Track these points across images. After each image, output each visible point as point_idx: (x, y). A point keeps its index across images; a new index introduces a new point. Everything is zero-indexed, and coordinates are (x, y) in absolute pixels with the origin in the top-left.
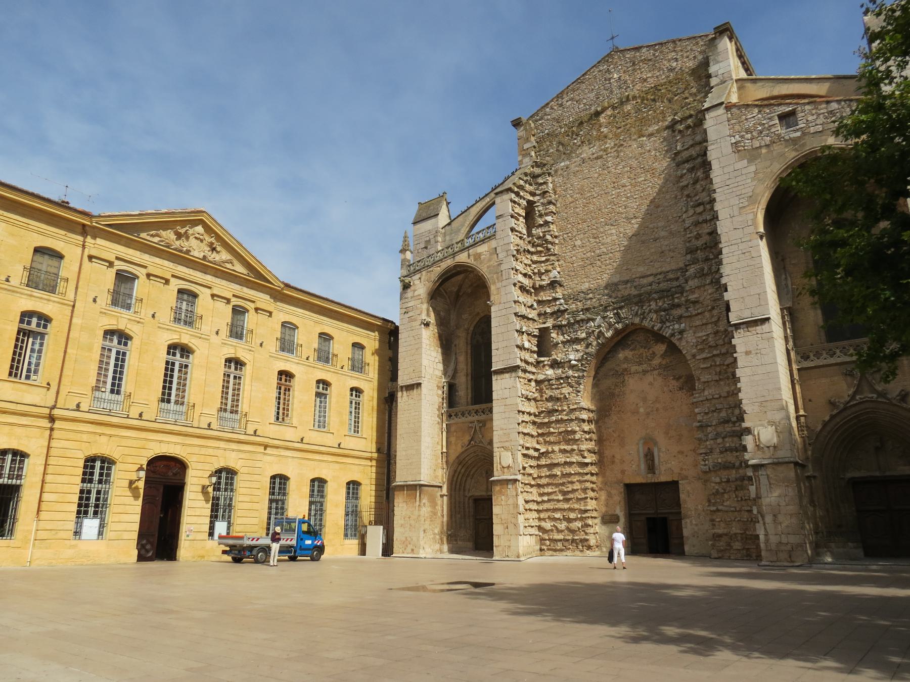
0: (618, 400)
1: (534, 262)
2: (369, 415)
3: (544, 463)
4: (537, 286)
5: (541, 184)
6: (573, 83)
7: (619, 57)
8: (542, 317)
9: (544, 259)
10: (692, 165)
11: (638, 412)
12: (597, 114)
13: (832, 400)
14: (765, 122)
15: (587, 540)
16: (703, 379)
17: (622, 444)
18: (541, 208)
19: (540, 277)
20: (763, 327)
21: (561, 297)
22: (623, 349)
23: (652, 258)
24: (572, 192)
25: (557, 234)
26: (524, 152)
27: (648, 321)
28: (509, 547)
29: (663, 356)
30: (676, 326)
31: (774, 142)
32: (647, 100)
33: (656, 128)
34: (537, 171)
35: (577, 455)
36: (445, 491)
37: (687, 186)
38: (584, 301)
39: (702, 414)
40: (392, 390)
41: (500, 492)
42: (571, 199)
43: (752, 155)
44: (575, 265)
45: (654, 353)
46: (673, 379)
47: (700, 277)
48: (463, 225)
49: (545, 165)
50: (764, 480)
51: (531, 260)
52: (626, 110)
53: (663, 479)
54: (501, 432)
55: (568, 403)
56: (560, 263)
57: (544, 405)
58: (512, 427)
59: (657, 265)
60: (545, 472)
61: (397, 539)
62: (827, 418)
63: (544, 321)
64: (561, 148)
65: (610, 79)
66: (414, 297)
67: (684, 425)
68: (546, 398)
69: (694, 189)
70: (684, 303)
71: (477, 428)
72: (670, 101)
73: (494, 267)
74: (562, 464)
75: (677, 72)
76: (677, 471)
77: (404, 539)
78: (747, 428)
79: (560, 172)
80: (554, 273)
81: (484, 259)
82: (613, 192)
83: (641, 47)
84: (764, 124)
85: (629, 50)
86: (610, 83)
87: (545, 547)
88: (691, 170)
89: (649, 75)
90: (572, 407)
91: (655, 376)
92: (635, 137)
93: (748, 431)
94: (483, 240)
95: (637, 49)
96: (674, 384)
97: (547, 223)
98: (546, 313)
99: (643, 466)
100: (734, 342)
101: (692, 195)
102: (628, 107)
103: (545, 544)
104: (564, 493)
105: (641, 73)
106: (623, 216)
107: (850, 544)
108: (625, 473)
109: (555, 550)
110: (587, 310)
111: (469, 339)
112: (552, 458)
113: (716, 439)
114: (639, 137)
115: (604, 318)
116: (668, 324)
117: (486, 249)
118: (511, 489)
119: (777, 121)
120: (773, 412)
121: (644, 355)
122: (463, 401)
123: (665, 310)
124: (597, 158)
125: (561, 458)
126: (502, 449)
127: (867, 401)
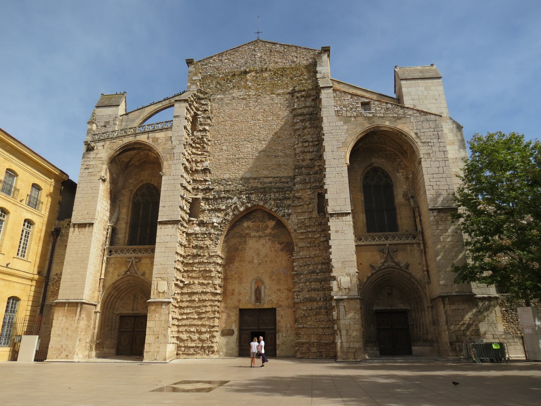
0: (240, 253)
1: (194, 154)
2: (36, 243)
3: (186, 292)
4: (194, 170)
5: (204, 105)
6: (230, 50)
7: (262, 45)
8: (195, 191)
9: (200, 153)
10: (303, 118)
11: (253, 262)
12: (246, 73)
13: (373, 265)
14: (354, 104)
15: (212, 347)
16: (300, 246)
17: (241, 282)
18: (201, 120)
19: (196, 164)
20: (347, 217)
21: (209, 180)
22: (247, 221)
23: (273, 167)
24: (223, 115)
25: (210, 139)
26: (192, 81)
27: (268, 205)
28: (158, 352)
29: (273, 229)
30: (286, 211)
31: (358, 116)
33: (282, 92)
34: (201, 96)
35: (211, 287)
36: (98, 309)
37: (299, 129)
38: (225, 185)
39: (298, 267)
40: (58, 227)
41: (155, 311)
42: (222, 119)
43: (347, 120)
44: (220, 161)
45: (267, 226)
46: (278, 244)
47: (303, 183)
48: (138, 118)
49: (206, 93)
51: (192, 152)
52: (264, 76)
53: (266, 306)
54: (160, 267)
55: (209, 251)
56: (210, 158)
57: (190, 251)
58: (170, 263)
59: (275, 172)
60: (186, 298)
62: (369, 275)
63: (196, 193)
64: (218, 86)
65: (255, 55)
67: (282, 273)
68: (192, 246)
69: (303, 132)
70: (292, 197)
71: (134, 262)
72: (291, 79)
73: (168, 149)
74: (199, 293)
75: (296, 64)
76: (275, 302)
77: (60, 346)
78: (333, 277)
81: (161, 143)
82: (252, 122)
83: (276, 43)
84: (353, 105)
85: (268, 42)
87: (180, 352)
88: (302, 121)
89: (280, 61)
90: (211, 254)
92: (269, 93)
93: (334, 278)
94: (161, 129)
95: (275, 44)
96: (278, 246)
97: (205, 130)
98: (198, 188)
99: (253, 298)
100: (329, 224)
101: (302, 135)
102: (266, 75)
103: (180, 350)
104: (199, 314)
105: (275, 58)
106: (257, 138)
108: (240, 302)
109: (188, 355)
110: (228, 191)
111: (132, 197)
112: (193, 289)
113: (306, 283)
114: (271, 94)
115: (239, 198)
116: (281, 209)
117: (164, 136)
118: (165, 309)
119: (360, 105)
120: (349, 268)
121: (261, 226)
122: (121, 242)
123: (280, 200)
124: (243, 99)
125: (199, 289)
126: (160, 279)
127: (390, 267)
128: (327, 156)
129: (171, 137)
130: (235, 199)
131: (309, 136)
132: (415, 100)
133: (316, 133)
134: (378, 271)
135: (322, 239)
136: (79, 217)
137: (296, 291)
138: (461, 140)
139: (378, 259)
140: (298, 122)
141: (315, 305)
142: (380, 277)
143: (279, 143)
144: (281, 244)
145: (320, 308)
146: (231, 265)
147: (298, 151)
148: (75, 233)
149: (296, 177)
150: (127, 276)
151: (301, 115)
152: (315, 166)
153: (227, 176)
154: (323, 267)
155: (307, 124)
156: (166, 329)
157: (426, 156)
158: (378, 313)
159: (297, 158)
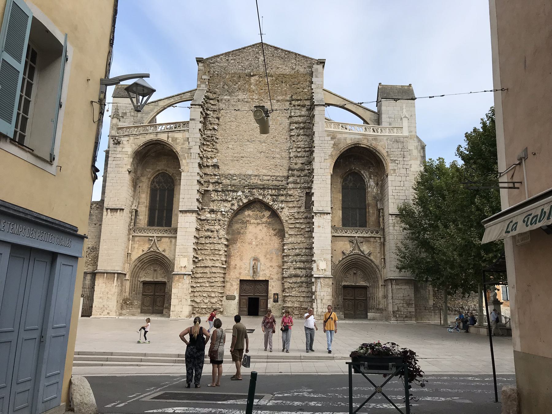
0: (242, 236)
4: (205, 165)
8: (206, 184)
9: (210, 150)
18: (210, 119)
19: (207, 160)
21: (218, 175)
24: (229, 116)
27: (266, 199)
29: (268, 217)
30: (280, 205)
32: (278, 80)
35: (220, 263)
37: (294, 135)
38: (231, 180)
41: (178, 281)
45: (264, 215)
46: (272, 230)
48: (152, 110)
50: (319, 284)
51: (203, 149)
53: (261, 279)
57: (203, 234)
58: (189, 244)
61: (95, 306)
62: (341, 259)
63: (207, 186)
64: (226, 87)
66: (122, 152)
68: (205, 230)
73: (185, 149)
76: (269, 275)
77: (102, 306)
79: (224, 101)
80: (215, 160)
82: (254, 125)
83: (278, 48)
86: (258, 61)
91: (263, 227)
97: (214, 129)
101: (296, 141)
107: (341, 313)
110: (234, 185)
111: (149, 184)
113: (293, 262)
115: (243, 192)
117: (181, 137)
121: (259, 215)
123: (275, 196)
125: (210, 264)
128: (316, 165)
129: (188, 138)
130: (240, 193)
131: (302, 143)
132: (391, 118)
133: (308, 140)
134: (348, 256)
135: (307, 230)
136: (110, 203)
137: (285, 268)
138: (423, 157)
139: (347, 247)
140: (294, 129)
141: (299, 280)
142: (348, 261)
143: (277, 146)
144: (274, 230)
145: (302, 282)
146: (234, 245)
147: (292, 155)
148: (108, 216)
149: (289, 177)
150: (150, 252)
151: (296, 123)
152: (305, 169)
153: (232, 172)
154: (306, 251)
155: (301, 132)
156: (187, 295)
157: (392, 172)
158: (345, 287)
159: (291, 161)
